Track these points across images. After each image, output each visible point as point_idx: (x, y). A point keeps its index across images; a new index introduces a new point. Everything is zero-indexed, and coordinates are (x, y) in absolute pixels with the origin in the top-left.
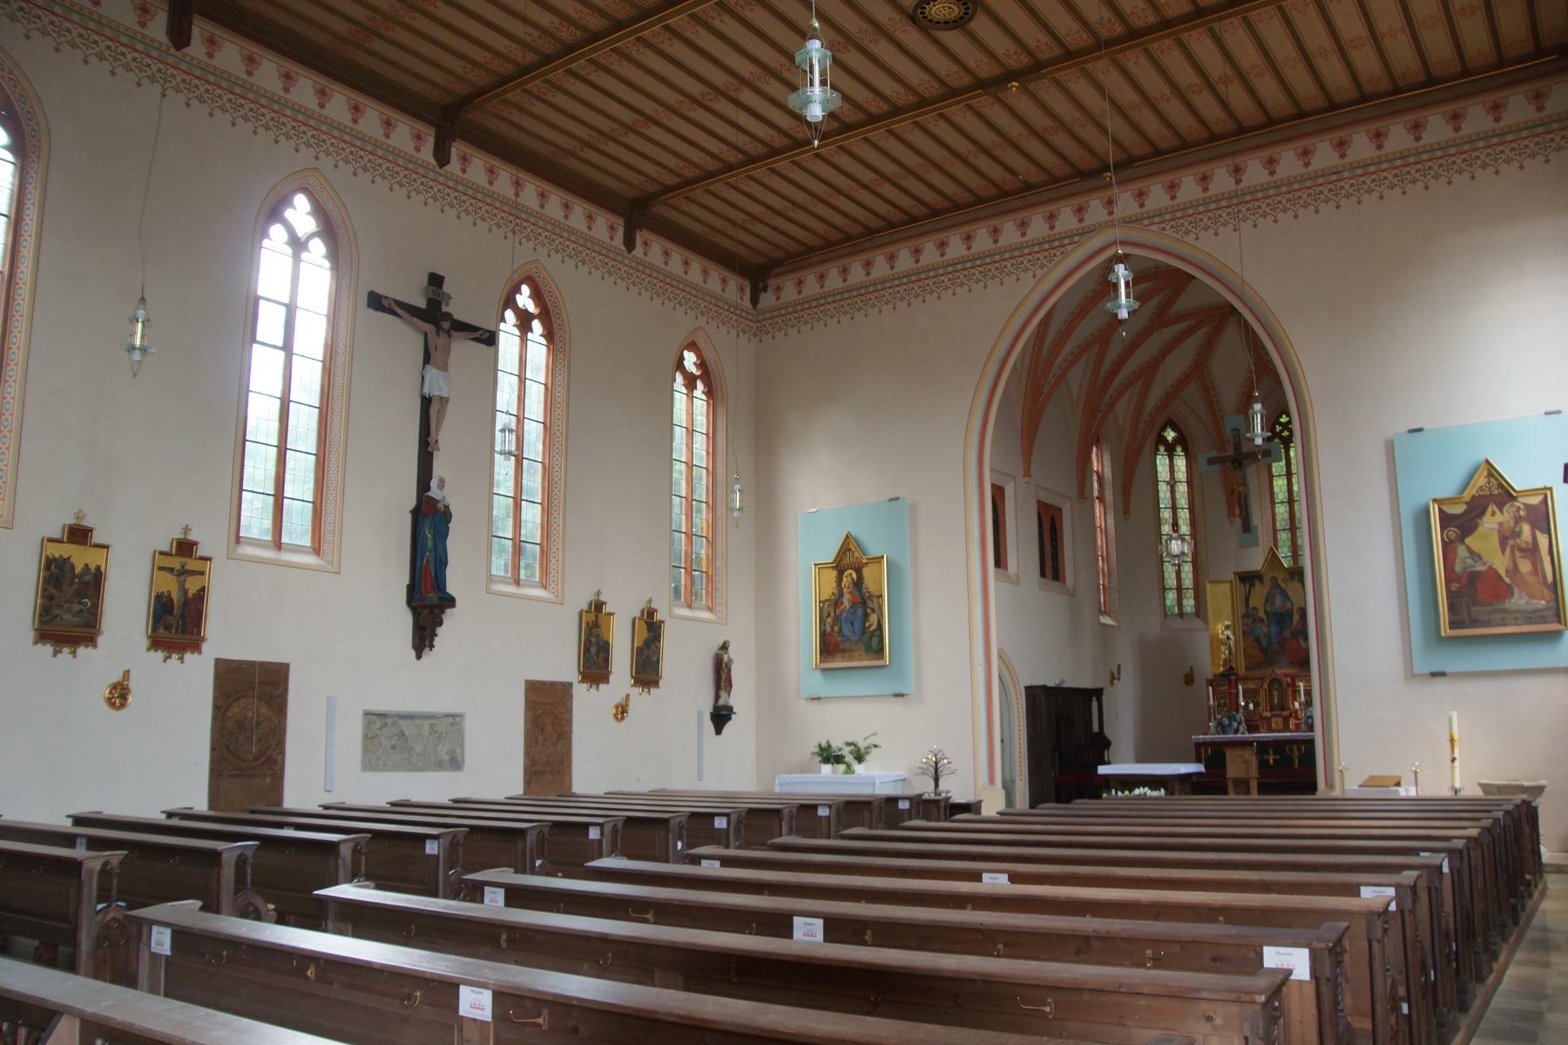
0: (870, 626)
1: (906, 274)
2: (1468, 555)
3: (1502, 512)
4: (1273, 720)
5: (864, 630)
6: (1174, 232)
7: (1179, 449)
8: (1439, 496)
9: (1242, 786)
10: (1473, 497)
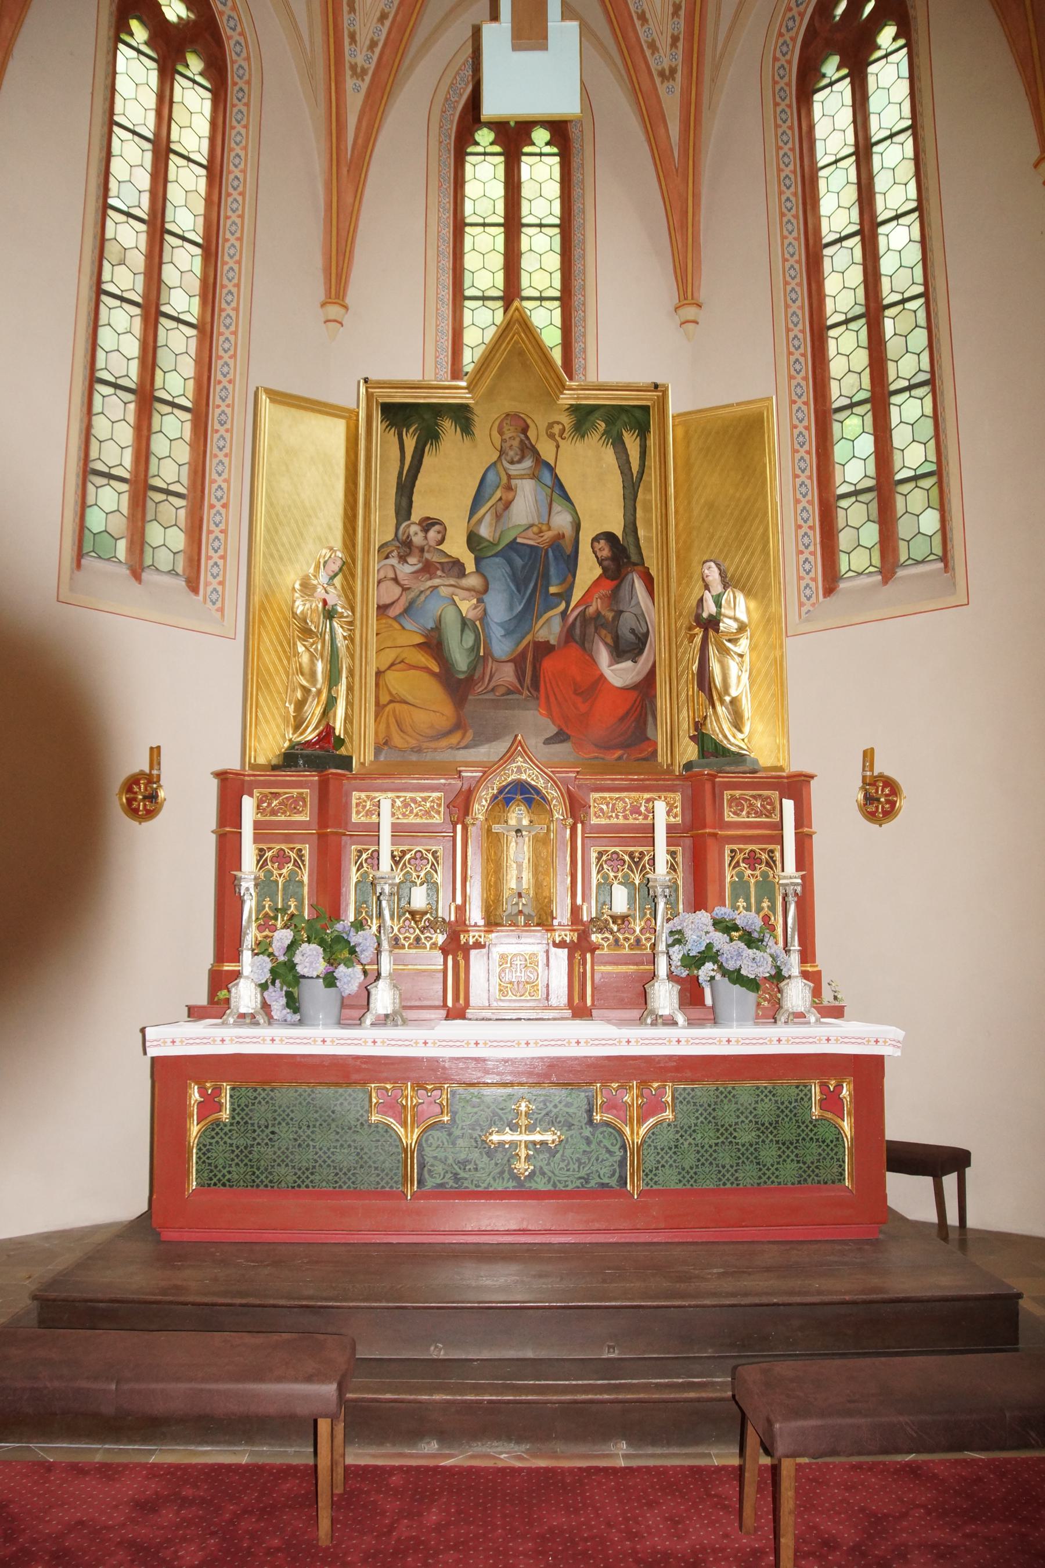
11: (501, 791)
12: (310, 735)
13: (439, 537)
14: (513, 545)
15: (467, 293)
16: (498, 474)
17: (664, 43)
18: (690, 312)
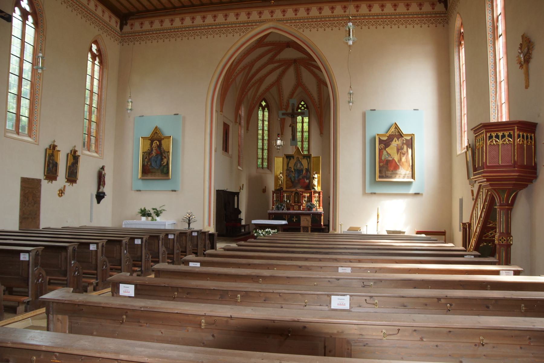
0: (164, 163)
1: (188, 27)
2: (386, 154)
3: (398, 141)
4: (295, 206)
5: (161, 165)
6: (295, 27)
7: (266, 109)
8: (379, 133)
9: (306, 229)
10: (390, 135)
18: (322, 135)
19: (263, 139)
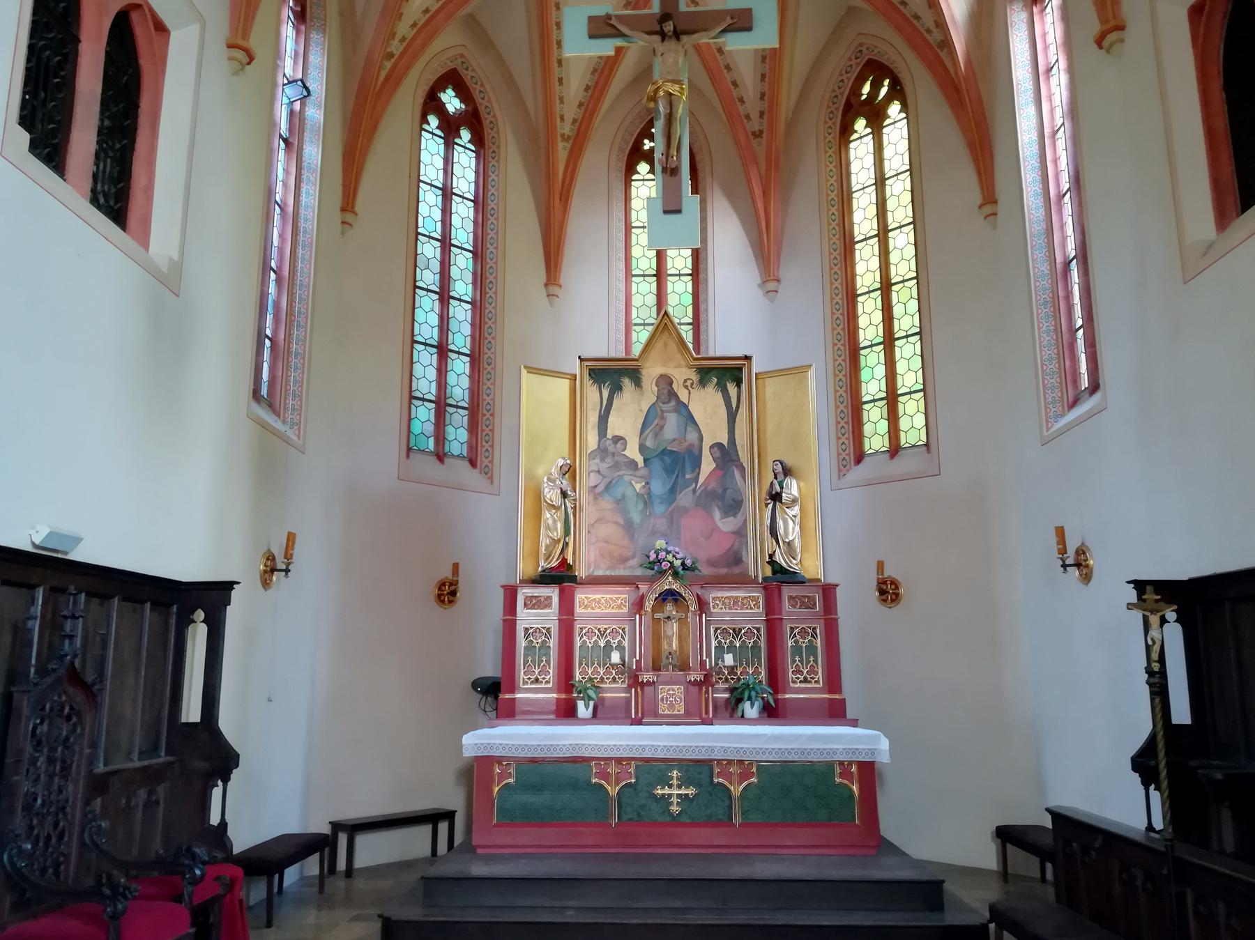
4: (663, 691)
7: (465, 135)
11: (660, 595)
12: (554, 564)
13: (623, 446)
14: (664, 452)
15: (634, 273)
16: (656, 409)
17: (755, 115)
18: (772, 286)
19: (444, 296)
